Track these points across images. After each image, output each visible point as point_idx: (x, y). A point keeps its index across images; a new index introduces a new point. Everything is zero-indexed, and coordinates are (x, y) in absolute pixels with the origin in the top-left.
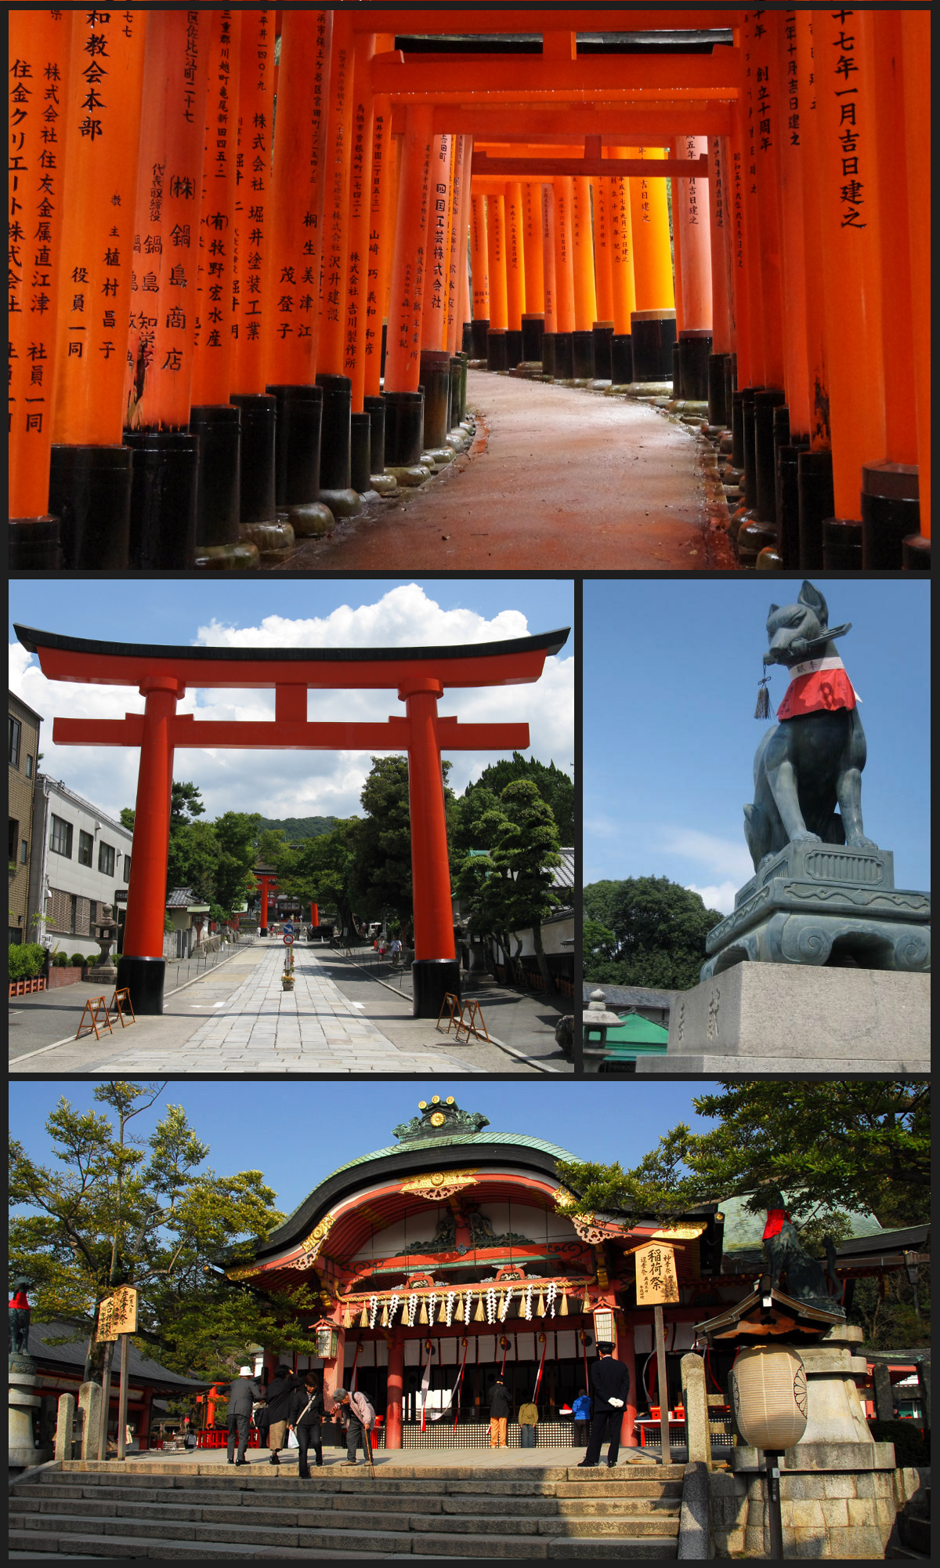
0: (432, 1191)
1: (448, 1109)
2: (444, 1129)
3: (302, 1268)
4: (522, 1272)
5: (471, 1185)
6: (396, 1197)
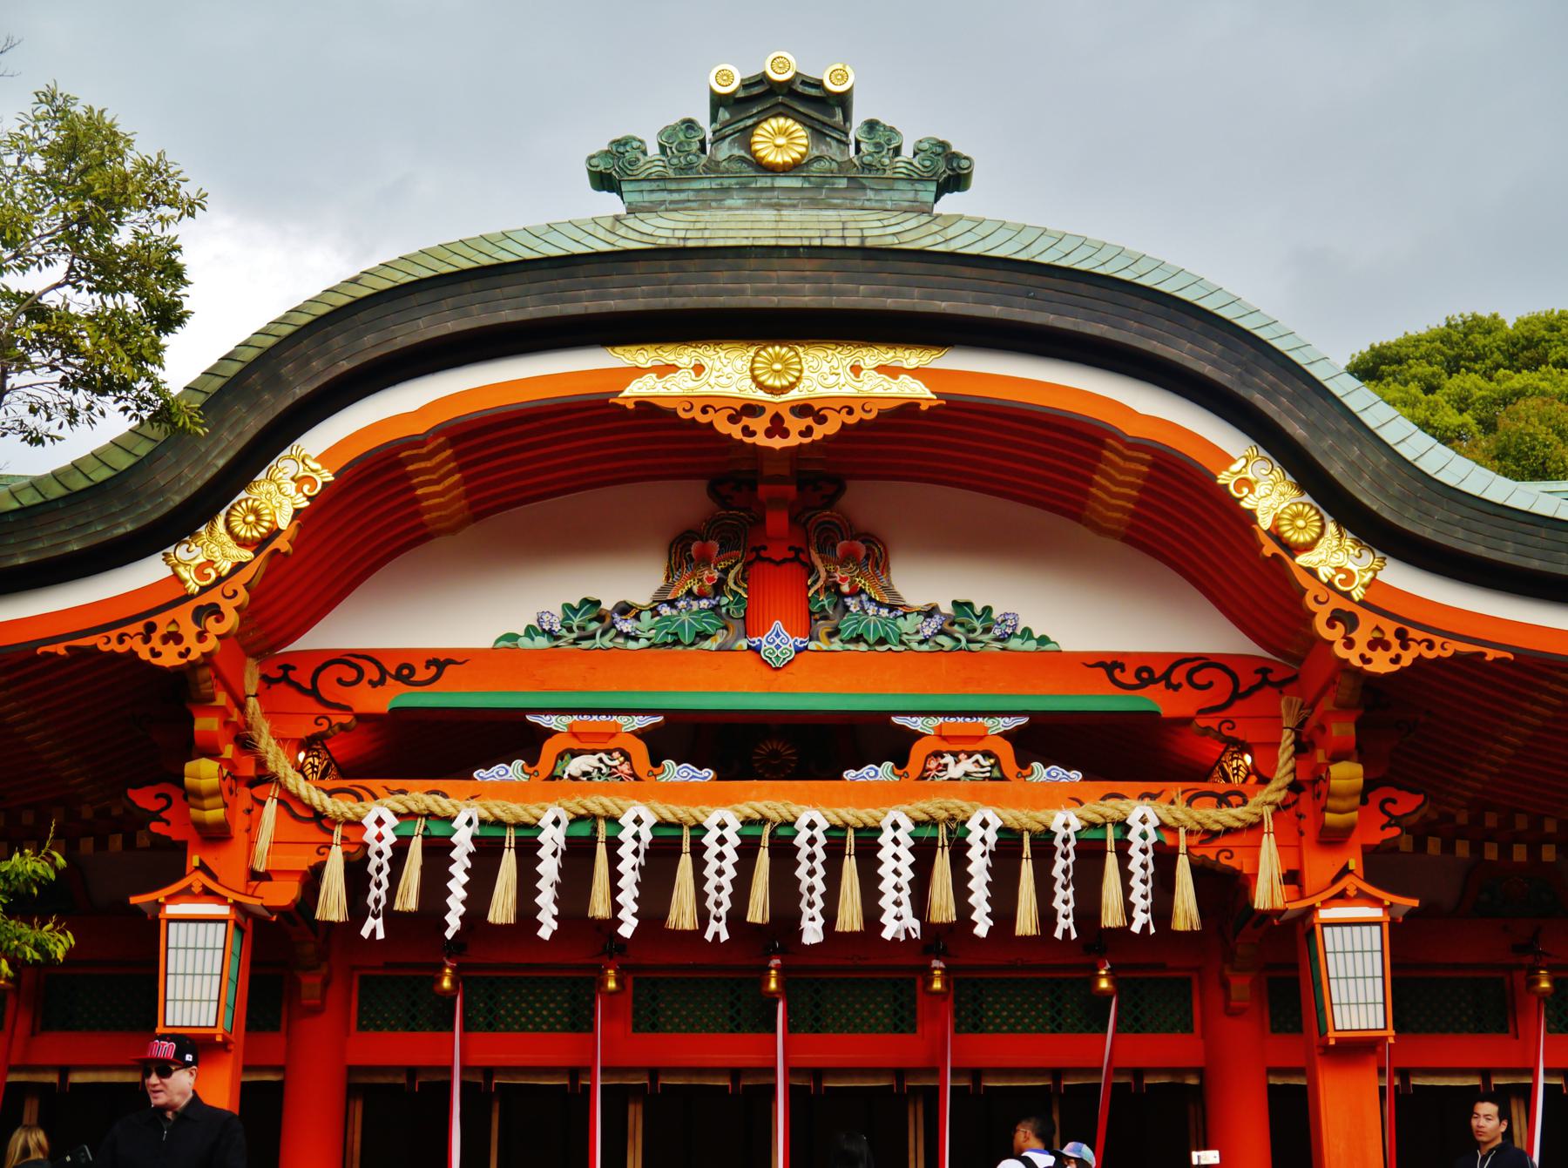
0: (752, 409)
1: (817, 105)
3: (169, 657)
4: (1006, 751)
5: (909, 409)
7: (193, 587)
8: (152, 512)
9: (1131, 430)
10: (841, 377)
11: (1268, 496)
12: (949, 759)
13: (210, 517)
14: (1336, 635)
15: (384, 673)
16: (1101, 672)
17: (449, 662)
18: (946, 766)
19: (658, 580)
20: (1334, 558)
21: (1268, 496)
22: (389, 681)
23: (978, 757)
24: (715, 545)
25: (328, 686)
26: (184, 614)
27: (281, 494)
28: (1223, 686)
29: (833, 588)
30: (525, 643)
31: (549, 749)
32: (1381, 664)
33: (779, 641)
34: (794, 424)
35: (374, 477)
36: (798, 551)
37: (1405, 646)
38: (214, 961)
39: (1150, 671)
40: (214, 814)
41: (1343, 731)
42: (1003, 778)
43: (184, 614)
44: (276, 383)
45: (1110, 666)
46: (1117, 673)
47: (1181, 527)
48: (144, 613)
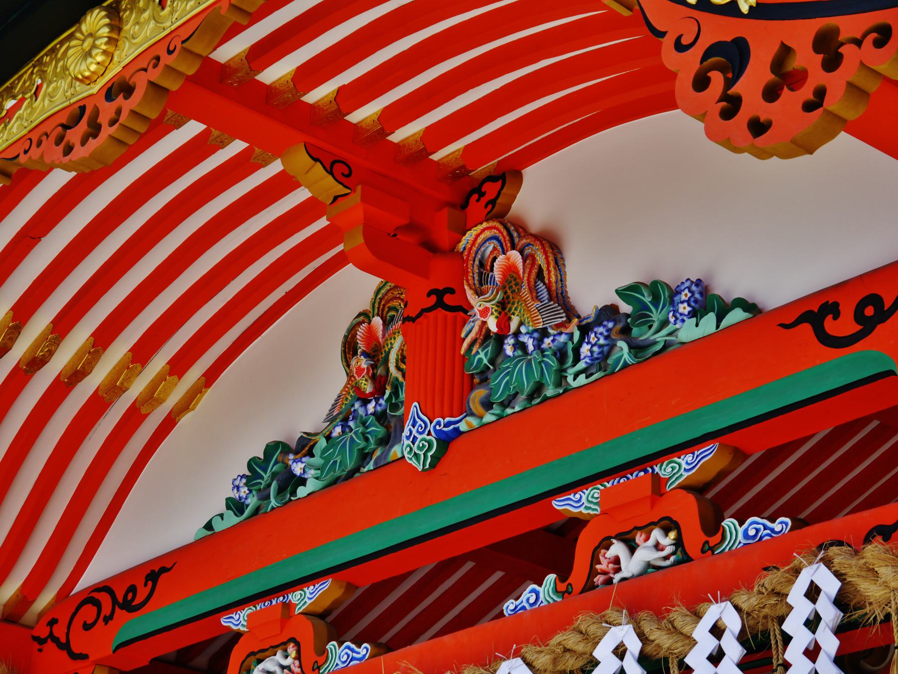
12: (617, 549)
15: (115, 601)
16: (806, 329)
17: (164, 570)
18: (617, 561)
22: (117, 610)
23: (656, 534)
24: (377, 321)
30: (219, 526)
36: (439, 294)
37: (832, 63)
39: (874, 300)
42: (686, 559)
46: (831, 326)
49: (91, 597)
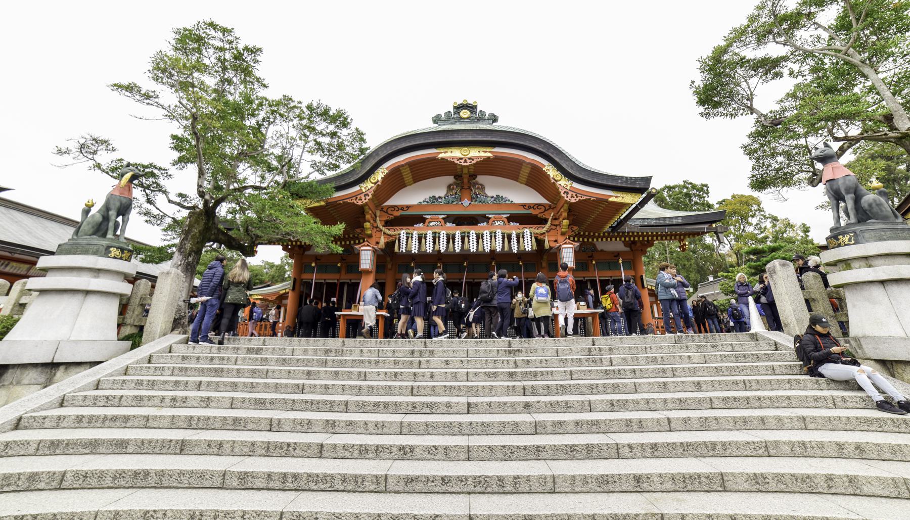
0: (461, 159)
2: (470, 120)
3: (360, 203)
4: (506, 220)
5: (489, 158)
6: (433, 160)
7: (364, 190)
8: (356, 177)
9: (528, 161)
10: (477, 154)
11: (552, 172)
13: (367, 179)
14: (565, 195)
19: (445, 192)
20: (564, 183)
21: (552, 172)
25: (389, 211)
26: (362, 196)
27: (379, 175)
28: (543, 209)
29: (475, 193)
31: (427, 221)
32: (573, 200)
33: (466, 202)
34: (468, 161)
35: (395, 173)
38: (369, 257)
40: (369, 232)
41: (565, 214)
43: (362, 196)
44: (377, 154)
45: (524, 205)
47: (537, 180)
48: (356, 196)
49: (394, 207)
